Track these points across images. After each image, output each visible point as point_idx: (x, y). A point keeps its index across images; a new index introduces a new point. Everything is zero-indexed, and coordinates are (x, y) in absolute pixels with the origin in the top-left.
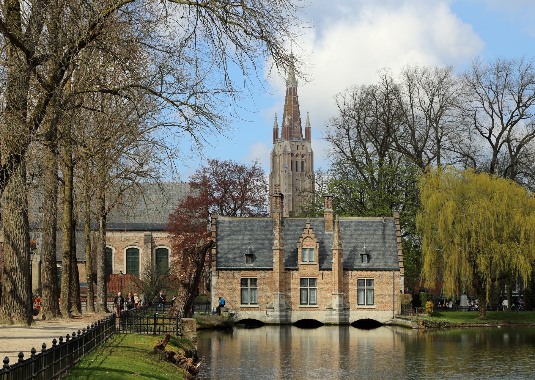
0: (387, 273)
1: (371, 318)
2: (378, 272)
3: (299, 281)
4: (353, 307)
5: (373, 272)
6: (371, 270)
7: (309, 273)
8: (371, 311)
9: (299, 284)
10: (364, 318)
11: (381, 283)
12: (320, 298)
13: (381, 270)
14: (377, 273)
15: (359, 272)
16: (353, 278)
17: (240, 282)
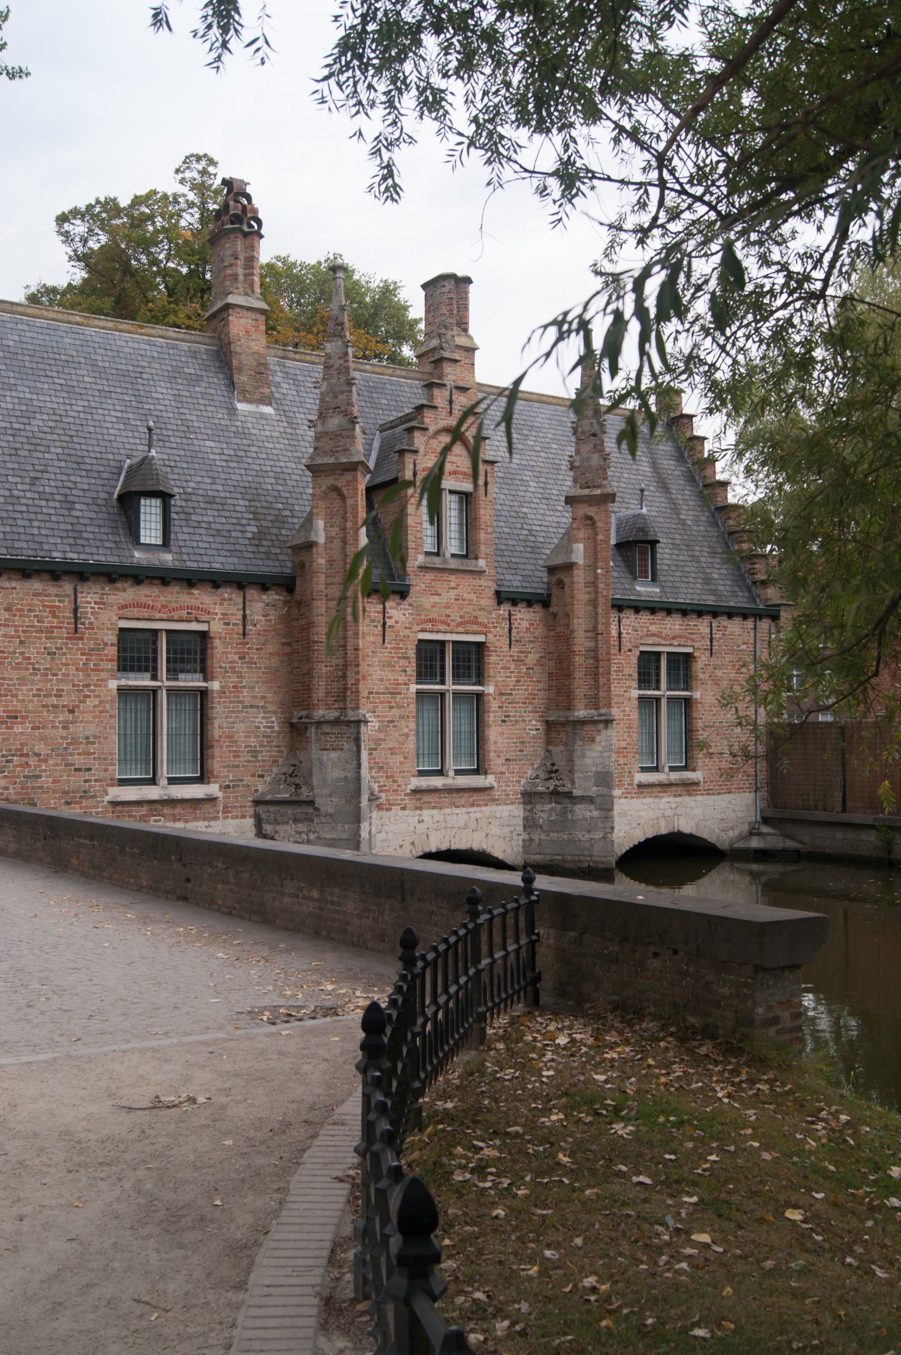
0: (735, 626)
1: (687, 827)
2: (706, 620)
3: (412, 653)
4: (626, 780)
5: (693, 621)
6: (684, 611)
7: (456, 617)
8: (687, 799)
9: (412, 669)
10: (664, 831)
11: (719, 673)
12: (500, 741)
13: (715, 613)
14: (702, 626)
15: (645, 618)
16: (626, 645)
17: (112, 651)
